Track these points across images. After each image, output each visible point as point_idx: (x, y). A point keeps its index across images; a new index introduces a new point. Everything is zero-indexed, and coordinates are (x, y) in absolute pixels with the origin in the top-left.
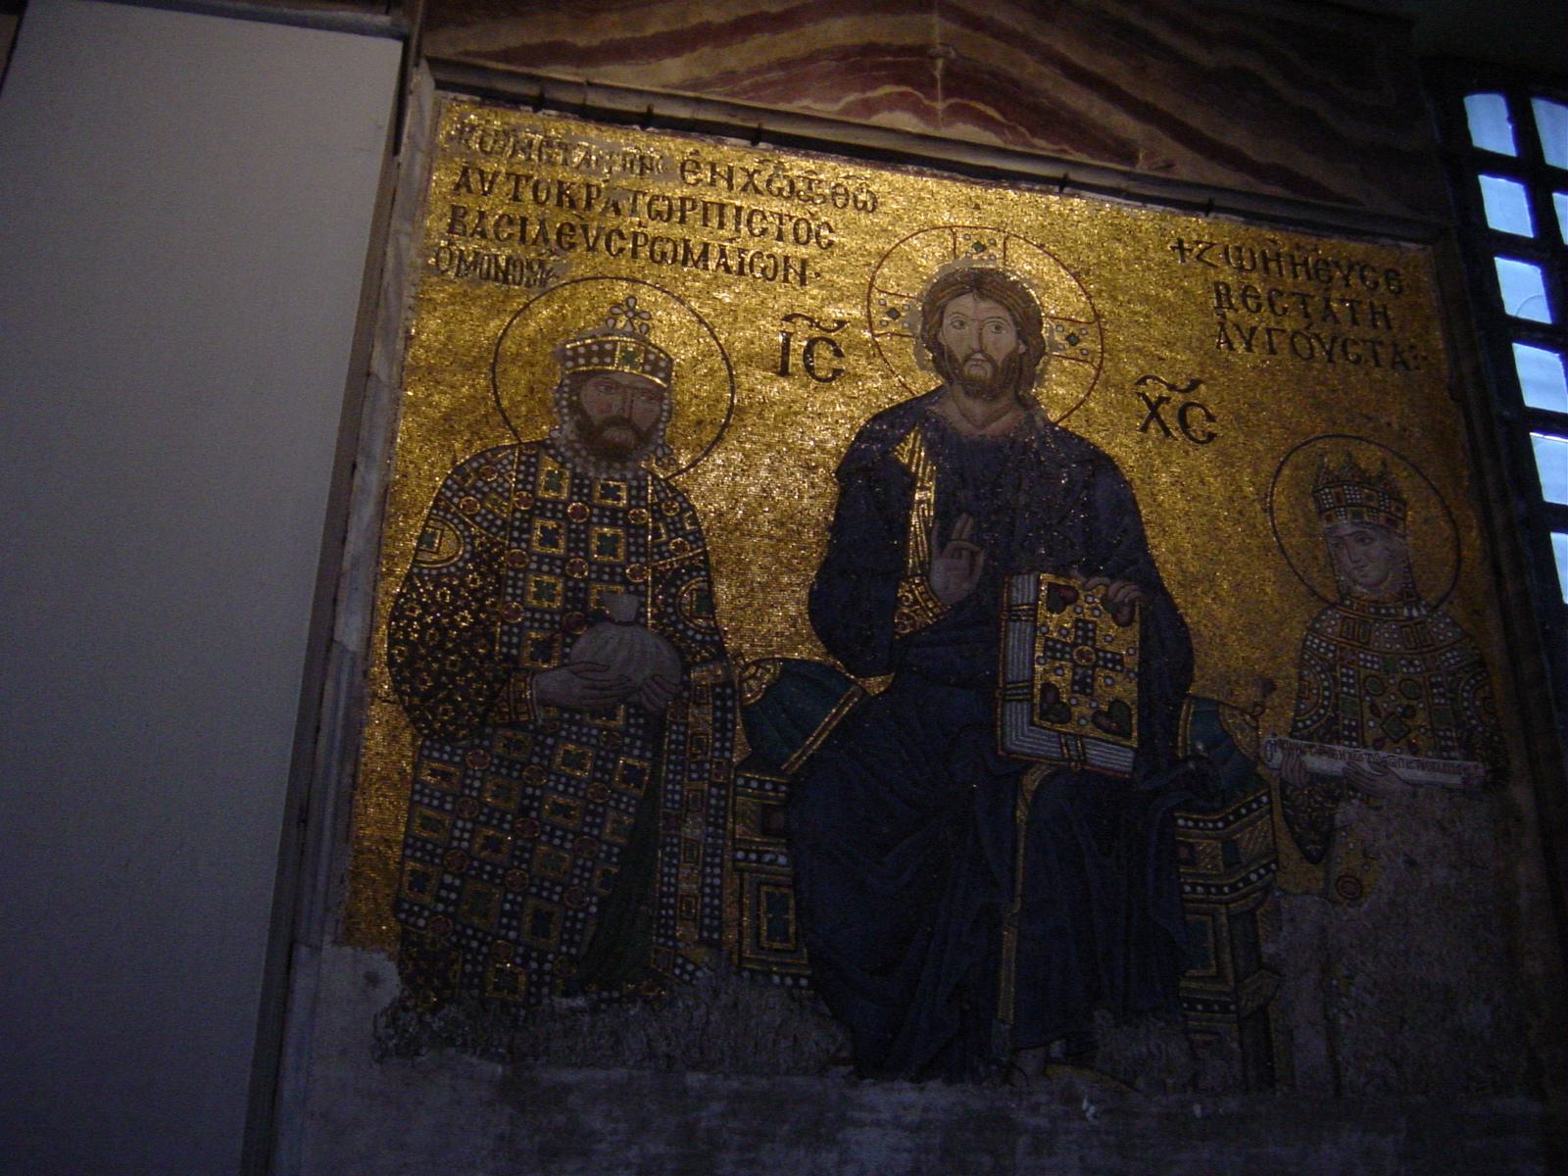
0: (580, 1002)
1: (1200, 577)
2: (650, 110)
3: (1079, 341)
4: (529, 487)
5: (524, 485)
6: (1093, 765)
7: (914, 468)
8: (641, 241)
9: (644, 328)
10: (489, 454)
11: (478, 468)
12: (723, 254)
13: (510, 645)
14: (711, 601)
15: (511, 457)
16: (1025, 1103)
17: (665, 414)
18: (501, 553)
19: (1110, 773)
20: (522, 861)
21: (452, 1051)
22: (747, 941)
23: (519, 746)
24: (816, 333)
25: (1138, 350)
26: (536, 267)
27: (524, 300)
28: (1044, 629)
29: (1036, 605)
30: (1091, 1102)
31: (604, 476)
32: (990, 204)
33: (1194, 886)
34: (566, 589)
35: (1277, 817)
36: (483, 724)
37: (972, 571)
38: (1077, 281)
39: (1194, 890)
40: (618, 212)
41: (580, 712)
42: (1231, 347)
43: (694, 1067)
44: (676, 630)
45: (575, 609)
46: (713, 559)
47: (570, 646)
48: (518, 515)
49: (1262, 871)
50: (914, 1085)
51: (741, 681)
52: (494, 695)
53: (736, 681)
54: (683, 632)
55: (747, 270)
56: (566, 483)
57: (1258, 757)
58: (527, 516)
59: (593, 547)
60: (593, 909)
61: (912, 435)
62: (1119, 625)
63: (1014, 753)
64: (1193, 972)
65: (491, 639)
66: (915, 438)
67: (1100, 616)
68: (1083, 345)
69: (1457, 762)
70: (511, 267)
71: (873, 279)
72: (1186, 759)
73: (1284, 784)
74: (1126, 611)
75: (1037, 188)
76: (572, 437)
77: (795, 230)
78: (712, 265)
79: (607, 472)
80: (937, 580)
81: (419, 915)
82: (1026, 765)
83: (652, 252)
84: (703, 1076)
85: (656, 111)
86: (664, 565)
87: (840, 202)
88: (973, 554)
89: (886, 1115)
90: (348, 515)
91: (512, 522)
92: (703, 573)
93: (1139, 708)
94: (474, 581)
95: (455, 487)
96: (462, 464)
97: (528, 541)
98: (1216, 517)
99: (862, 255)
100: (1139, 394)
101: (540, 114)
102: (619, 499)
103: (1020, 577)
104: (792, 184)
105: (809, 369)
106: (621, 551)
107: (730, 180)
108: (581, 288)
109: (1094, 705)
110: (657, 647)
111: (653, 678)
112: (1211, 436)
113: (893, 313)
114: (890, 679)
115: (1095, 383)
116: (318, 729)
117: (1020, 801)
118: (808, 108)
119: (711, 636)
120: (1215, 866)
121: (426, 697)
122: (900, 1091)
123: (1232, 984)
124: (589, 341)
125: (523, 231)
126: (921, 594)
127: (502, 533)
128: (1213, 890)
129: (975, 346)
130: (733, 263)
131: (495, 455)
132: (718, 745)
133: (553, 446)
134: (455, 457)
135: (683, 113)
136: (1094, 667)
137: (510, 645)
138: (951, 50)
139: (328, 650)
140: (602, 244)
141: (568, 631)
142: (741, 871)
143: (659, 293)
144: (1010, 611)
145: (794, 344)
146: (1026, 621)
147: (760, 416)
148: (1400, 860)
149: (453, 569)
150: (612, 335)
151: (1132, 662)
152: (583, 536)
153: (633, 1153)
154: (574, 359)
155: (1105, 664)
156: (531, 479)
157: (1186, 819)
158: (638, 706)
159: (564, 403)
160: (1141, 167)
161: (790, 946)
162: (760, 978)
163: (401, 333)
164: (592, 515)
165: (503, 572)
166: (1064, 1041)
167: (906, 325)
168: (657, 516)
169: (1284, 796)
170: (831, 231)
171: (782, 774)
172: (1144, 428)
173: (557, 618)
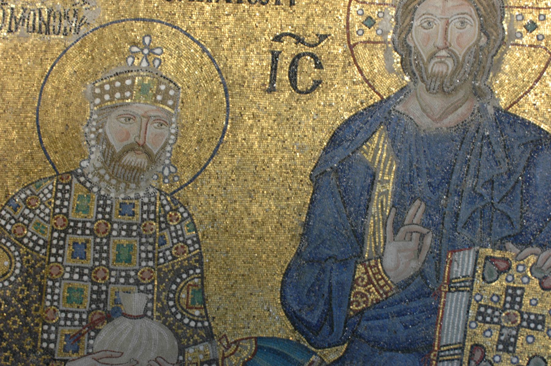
4: (64, 210)
5: (61, 210)
9: (157, 63)
10: (32, 187)
11: (26, 198)
13: (49, 341)
14: (203, 294)
15: (50, 187)
17: (173, 137)
18: (43, 267)
24: (302, 49)
26: (71, 16)
27: (62, 46)
28: (478, 298)
29: (474, 276)
31: (122, 196)
34: (93, 292)
37: (420, 250)
44: (176, 320)
45: (98, 308)
46: (206, 260)
47: (94, 338)
48: (56, 235)
51: (224, 358)
53: (220, 357)
54: (181, 320)
56: (94, 208)
58: (63, 235)
59: (112, 257)
61: (377, 134)
62: (543, 289)
65: (34, 336)
66: (380, 137)
67: (528, 283)
70: (52, 18)
76: (98, 165)
79: (125, 192)
80: (390, 260)
86: (167, 267)
88: (422, 236)
91: (51, 241)
92: (198, 271)
94: (22, 291)
95: (8, 216)
96: (14, 196)
97: (62, 256)
102: (133, 214)
103: (462, 253)
106: (135, 258)
108: (107, 31)
109: (515, 360)
110: (160, 333)
119: (202, 322)
124: (113, 78)
126: (374, 274)
127: (44, 251)
129: (440, 43)
131: (38, 187)
133: (83, 175)
134: (7, 191)
136: (520, 326)
137: (49, 341)
143: (170, 29)
146: (463, 291)
149: (6, 283)
150: (132, 71)
152: (105, 248)
154: (101, 96)
155: (529, 324)
156: (66, 203)
159: (92, 136)
164: (112, 229)
165: (43, 282)
167: (379, 32)
168: (163, 226)
173: (84, 316)
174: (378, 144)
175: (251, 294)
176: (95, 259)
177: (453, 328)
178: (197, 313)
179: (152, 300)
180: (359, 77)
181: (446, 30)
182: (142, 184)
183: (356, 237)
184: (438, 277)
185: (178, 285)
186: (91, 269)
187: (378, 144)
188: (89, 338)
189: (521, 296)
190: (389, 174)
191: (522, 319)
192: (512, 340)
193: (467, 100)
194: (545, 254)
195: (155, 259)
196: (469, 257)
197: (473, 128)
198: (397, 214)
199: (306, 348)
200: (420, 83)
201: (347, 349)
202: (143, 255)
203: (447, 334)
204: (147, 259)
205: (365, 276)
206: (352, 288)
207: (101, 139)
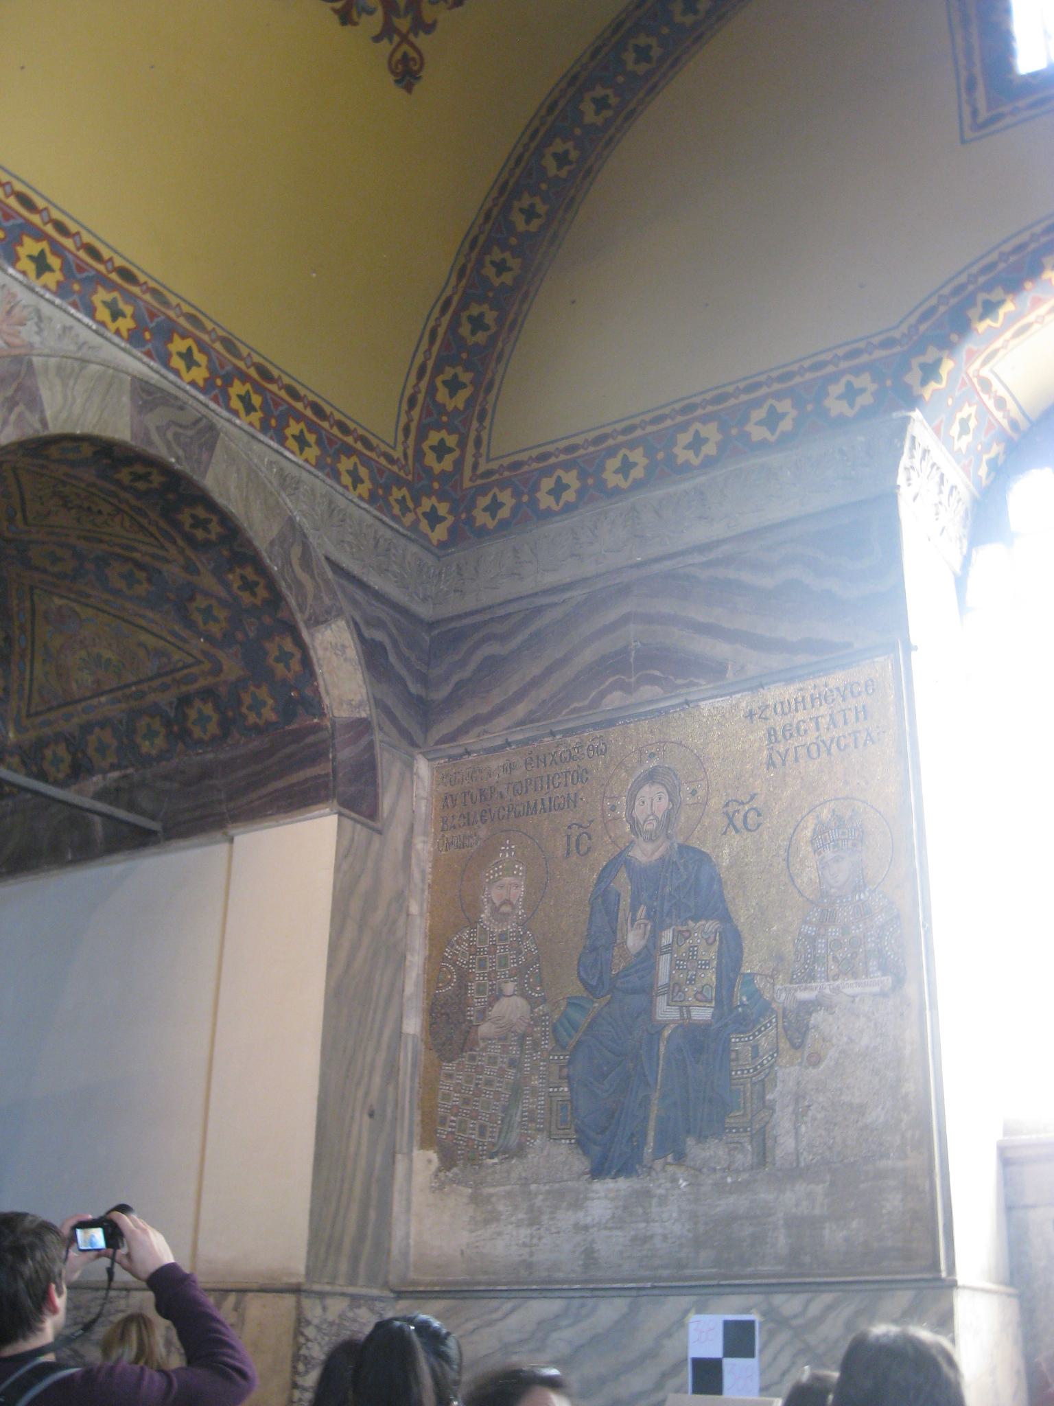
0: (496, 1160)
2: (507, 739)
6: (695, 1020)
8: (511, 809)
12: (543, 804)
13: (471, 1016)
19: (701, 1022)
20: (476, 1106)
21: (454, 1185)
22: (553, 1127)
23: (473, 1058)
30: (685, 1180)
31: (500, 930)
33: (736, 1071)
35: (780, 1029)
36: (462, 1051)
40: (502, 797)
41: (495, 1039)
43: (535, 1182)
49: (770, 1058)
50: (614, 1180)
52: (465, 1039)
54: (531, 994)
55: (553, 808)
57: (773, 999)
60: (499, 1122)
64: (732, 1115)
69: (877, 979)
73: (784, 1012)
74: (713, 935)
75: (678, 709)
76: (489, 915)
78: (538, 812)
81: (443, 1134)
82: (665, 1025)
83: (515, 813)
84: (535, 1185)
85: (509, 740)
88: (646, 925)
90: (404, 978)
95: (449, 951)
100: (724, 813)
101: (471, 758)
104: (570, 755)
105: (579, 853)
107: (545, 763)
111: (520, 1019)
116: (399, 1069)
117: (661, 1044)
118: (575, 710)
121: (444, 1044)
122: (607, 1183)
123: (749, 1117)
125: (469, 819)
130: (547, 803)
131: (463, 932)
132: (543, 1043)
135: (520, 737)
137: (471, 1016)
138: (639, 643)
139: (400, 1037)
140: (496, 816)
141: (491, 1004)
142: (551, 1097)
148: (845, 1039)
151: (715, 963)
153: (513, 1219)
154: (488, 877)
158: (515, 1032)
159: (486, 900)
160: (729, 674)
162: (557, 1141)
163: (426, 887)
169: (784, 1016)
170: (587, 773)
172: (725, 833)
176: (490, 967)
178: (538, 989)
179: (517, 985)
182: (509, 922)
183: (613, 932)
184: (655, 948)
185: (528, 974)
186: (489, 973)
188: (490, 1011)
189: (697, 951)
194: (708, 924)
195: (517, 962)
197: (667, 858)
198: (632, 915)
201: (612, 997)
202: (512, 961)
204: (514, 963)
207: (490, 900)
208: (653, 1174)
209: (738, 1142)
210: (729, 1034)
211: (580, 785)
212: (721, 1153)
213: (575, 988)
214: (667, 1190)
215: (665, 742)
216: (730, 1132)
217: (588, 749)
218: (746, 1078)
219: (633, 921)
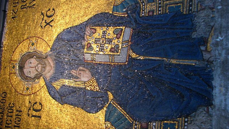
1: (84, 11)
3: (33, 43)
7: (61, 85)
16: (218, 57)
24: (32, 109)
25: (35, 28)
30: (217, 38)
32: (5, 64)
33: (159, 11)
38: (20, 43)
39: (160, 11)
42: (34, 5)
55: (18, 125)
61: (54, 85)
62: (95, 33)
63: (127, 61)
66: (54, 84)
68: (34, 42)
71: (20, 94)
72: (127, 13)
74: (93, 30)
75: (1, 53)
77: (10, 112)
80: (85, 79)
87: (4, 101)
88: (80, 70)
89: (223, 98)
93: (115, 27)
98: (71, 8)
99: (15, 96)
105: (39, 110)
109: (114, 38)
112: (53, 9)
113: (28, 89)
114: (109, 93)
115: (42, 39)
120: (154, 5)
122: (216, 93)
128: (160, 5)
136: (105, 38)
144: (92, 61)
145: (34, 114)
147: (49, 123)
157: (142, 13)
161: (177, 123)
166: (200, 46)
170: (10, 104)
171: (133, 122)
172: (52, 26)
174: (56, 85)
175: (92, 123)
177: (105, 58)
180: (40, 91)
181: (32, 67)
187: (56, 85)
189: (97, 39)
190: (63, 81)
191: (104, 38)
192: (109, 40)
193: (47, 60)
196: (86, 56)
197: (54, 57)
199: (108, 105)
200: (43, 74)
203: (107, 60)
205: (90, 87)
206: (93, 91)
208: (211, 59)
209: (198, 4)
210: (140, 17)
211: (14, 108)
212: (203, 15)
213: (101, 115)
214: (223, 49)
215: (11, 60)
216: (191, 10)
217: (2, 103)
218: (163, 4)
219: (77, 78)
